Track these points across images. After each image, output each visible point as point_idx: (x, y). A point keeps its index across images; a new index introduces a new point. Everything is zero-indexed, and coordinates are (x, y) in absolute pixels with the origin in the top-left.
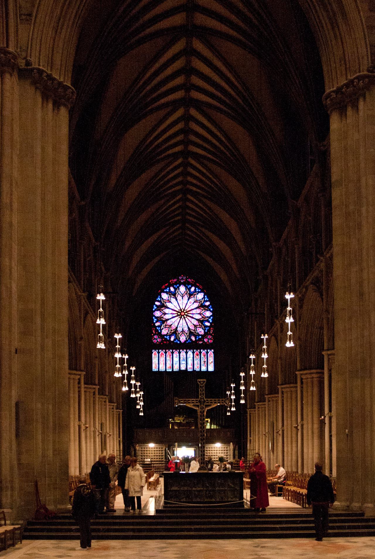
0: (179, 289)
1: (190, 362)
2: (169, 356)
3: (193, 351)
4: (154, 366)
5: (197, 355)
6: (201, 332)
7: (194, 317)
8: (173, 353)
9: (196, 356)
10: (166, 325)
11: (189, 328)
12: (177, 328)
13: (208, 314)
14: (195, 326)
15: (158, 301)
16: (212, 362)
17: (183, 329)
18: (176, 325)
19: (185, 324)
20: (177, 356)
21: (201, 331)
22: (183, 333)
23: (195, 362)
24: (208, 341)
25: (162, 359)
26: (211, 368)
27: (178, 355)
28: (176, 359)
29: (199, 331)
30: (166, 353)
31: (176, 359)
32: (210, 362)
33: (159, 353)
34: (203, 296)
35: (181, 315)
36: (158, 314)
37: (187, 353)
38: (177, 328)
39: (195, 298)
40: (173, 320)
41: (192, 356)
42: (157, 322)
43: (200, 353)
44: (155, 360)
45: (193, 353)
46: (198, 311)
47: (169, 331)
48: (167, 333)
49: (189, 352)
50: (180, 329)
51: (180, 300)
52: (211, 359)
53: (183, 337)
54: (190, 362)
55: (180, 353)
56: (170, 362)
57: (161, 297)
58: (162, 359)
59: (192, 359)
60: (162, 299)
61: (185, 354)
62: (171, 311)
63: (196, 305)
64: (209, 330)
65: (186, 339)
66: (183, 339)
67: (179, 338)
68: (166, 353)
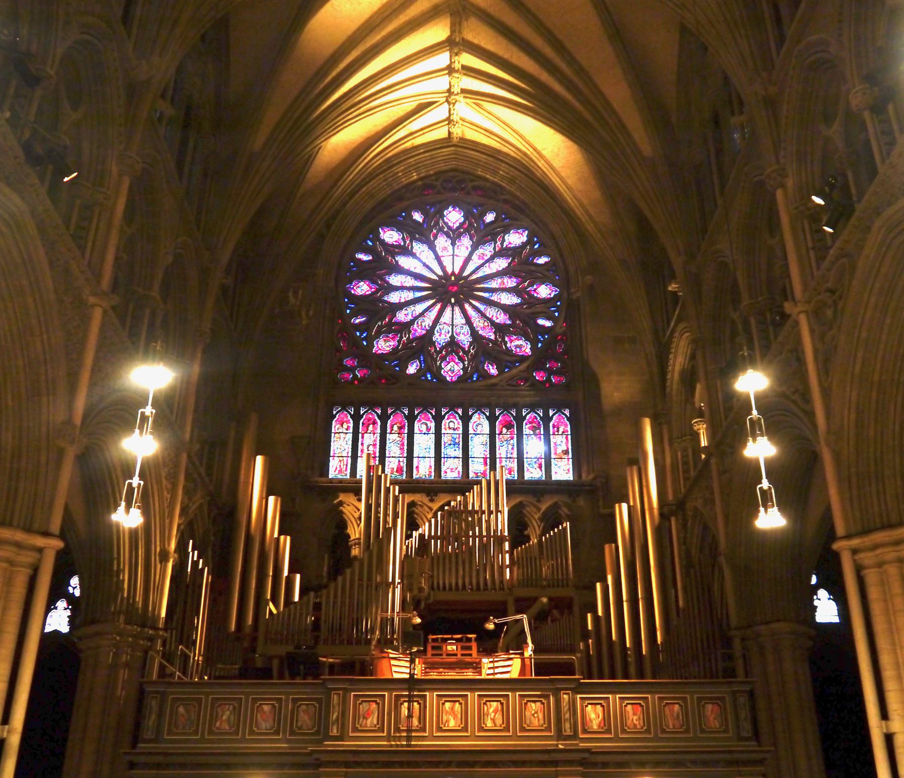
0: (442, 216)
1: (478, 447)
2: (395, 428)
3: (492, 413)
4: (334, 464)
5: (508, 426)
6: (520, 347)
7: (495, 297)
8: (411, 419)
9: (504, 430)
10: (390, 324)
11: (474, 332)
12: (431, 331)
13: (544, 291)
14: (500, 329)
15: (366, 251)
16: (566, 452)
17: (452, 337)
18: (428, 321)
19: (459, 319)
20: (428, 429)
21: (521, 346)
22: (453, 351)
23: (501, 452)
24: (549, 380)
25: (369, 439)
26: (563, 471)
27: (432, 425)
28: (424, 443)
29: (513, 344)
30: (384, 418)
31: (424, 443)
32: (559, 451)
33: (356, 418)
34: (525, 239)
35: (446, 293)
36: (363, 288)
37: (466, 419)
38: (431, 331)
39: (499, 243)
40: (420, 308)
41: (485, 427)
42: (355, 314)
43: (520, 419)
44: (340, 444)
45: (492, 420)
46: (511, 283)
47: (399, 342)
48: (395, 350)
49: (475, 418)
50: (441, 338)
51: (445, 249)
52: (561, 442)
53: (452, 364)
54: (478, 447)
55: (438, 419)
56: (402, 449)
57: (377, 238)
58: (369, 439)
59: (486, 439)
60: (383, 243)
61: (458, 424)
62: (409, 282)
63: (501, 264)
64: (548, 345)
65: (464, 369)
66: (452, 369)
67: (440, 368)
68: (384, 418)
